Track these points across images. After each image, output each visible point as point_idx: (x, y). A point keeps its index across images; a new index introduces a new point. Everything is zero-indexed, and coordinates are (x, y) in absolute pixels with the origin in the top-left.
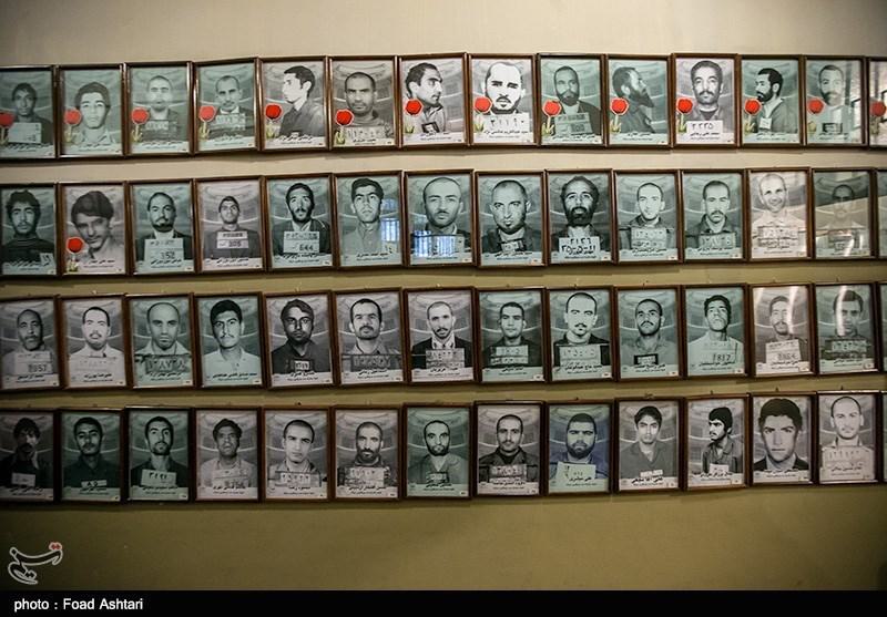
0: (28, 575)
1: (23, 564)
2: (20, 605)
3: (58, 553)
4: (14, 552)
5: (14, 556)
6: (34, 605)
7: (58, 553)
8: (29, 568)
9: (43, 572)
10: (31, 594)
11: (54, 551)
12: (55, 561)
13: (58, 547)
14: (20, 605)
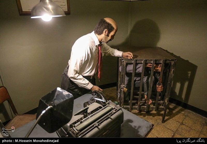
1: (5, 132)
3: (13, 129)
4: (3, 129)
5: (3, 130)
7: (13, 129)
8: (7, 133)
10: (7, 139)
11: (12, 129)
13: (14, 128)
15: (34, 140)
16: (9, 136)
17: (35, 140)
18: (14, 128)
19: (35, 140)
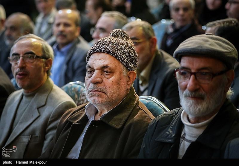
0: (7, 155)
2: (4, 163)
3: (15, 149)
4: (3, 148)
5: (3, 150)
6: (8, 163)
7: (15, 149)
9: (11, 154)
10: (8, 160)
11: (14, 148)
12: (15, 151)
13: (15, 147)
14: (4, 163)
15: (31, 161)
16: (9, 157)
17: (32, 161)
18: (16, 148)
19: (32, 161)
